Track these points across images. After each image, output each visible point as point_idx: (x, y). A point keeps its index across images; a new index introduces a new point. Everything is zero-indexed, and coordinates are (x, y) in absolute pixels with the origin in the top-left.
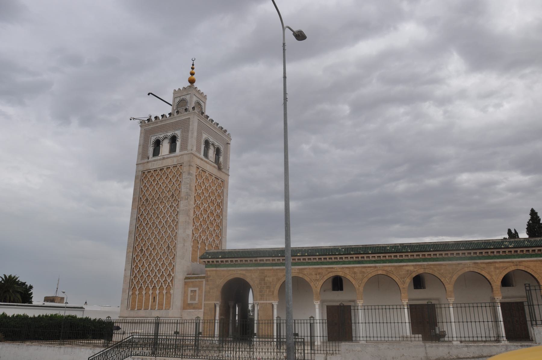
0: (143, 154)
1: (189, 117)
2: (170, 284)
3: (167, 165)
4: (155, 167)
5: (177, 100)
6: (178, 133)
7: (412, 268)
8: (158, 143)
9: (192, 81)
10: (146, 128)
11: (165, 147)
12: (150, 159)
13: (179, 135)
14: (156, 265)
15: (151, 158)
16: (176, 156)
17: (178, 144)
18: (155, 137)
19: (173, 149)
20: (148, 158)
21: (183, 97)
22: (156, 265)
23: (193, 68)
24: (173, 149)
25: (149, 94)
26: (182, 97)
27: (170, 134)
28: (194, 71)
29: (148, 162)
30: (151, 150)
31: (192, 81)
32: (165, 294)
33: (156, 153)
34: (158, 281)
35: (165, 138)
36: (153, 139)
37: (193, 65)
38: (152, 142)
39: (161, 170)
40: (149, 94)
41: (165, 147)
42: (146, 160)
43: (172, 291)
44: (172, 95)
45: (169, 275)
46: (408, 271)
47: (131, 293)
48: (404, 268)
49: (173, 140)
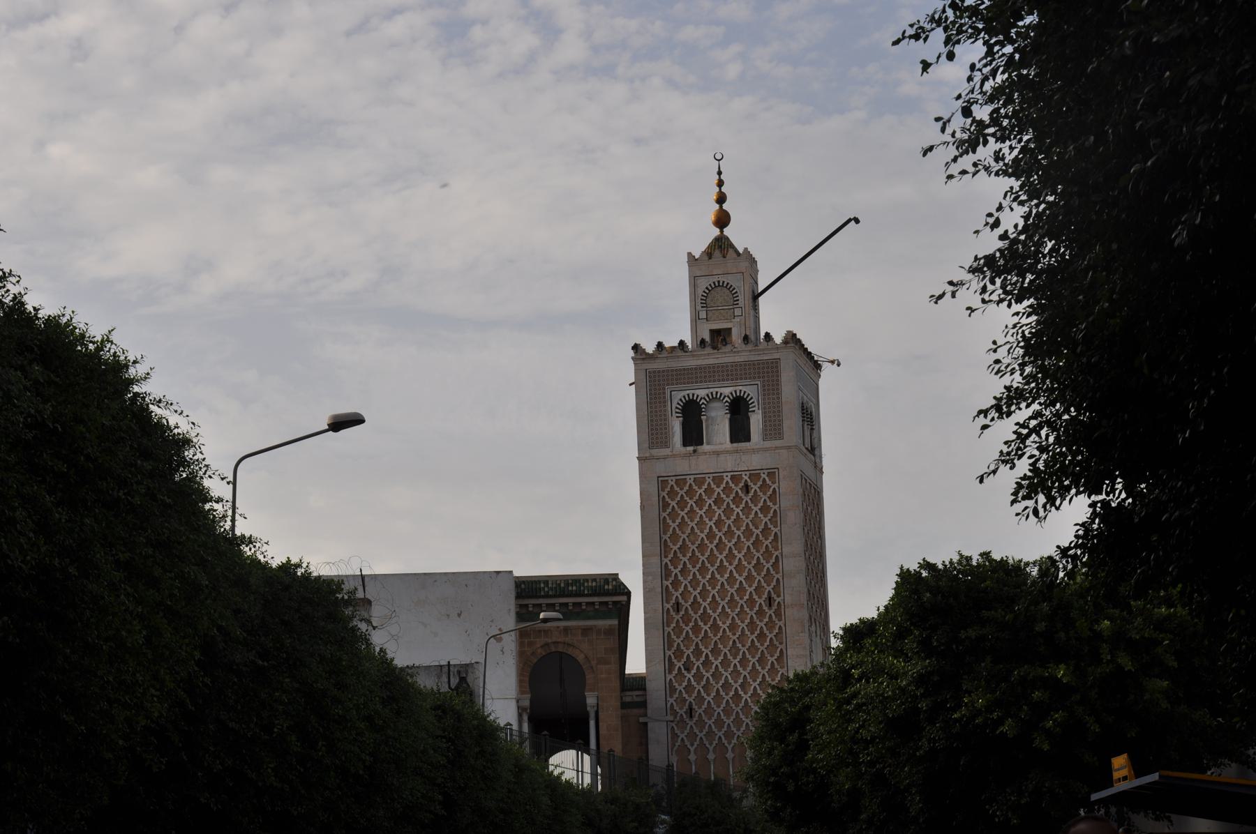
0: (652, 434)
1: (776, 356)
6: (750, 390)
8: (692, 414)
9: (722, 220)
11: (718, 424)
16: (754, 451)
17: (756, 421)
19: (740, 432)
23: (720, 183)
24: (740, 432)
28: (723, 189)
29: (674, 456)
30: (676, 426)
31: (722, 220)
33: (693, 435)
36: (679, 396)
37: (720, 173)
41: (718, 424)
49: (738, 408)
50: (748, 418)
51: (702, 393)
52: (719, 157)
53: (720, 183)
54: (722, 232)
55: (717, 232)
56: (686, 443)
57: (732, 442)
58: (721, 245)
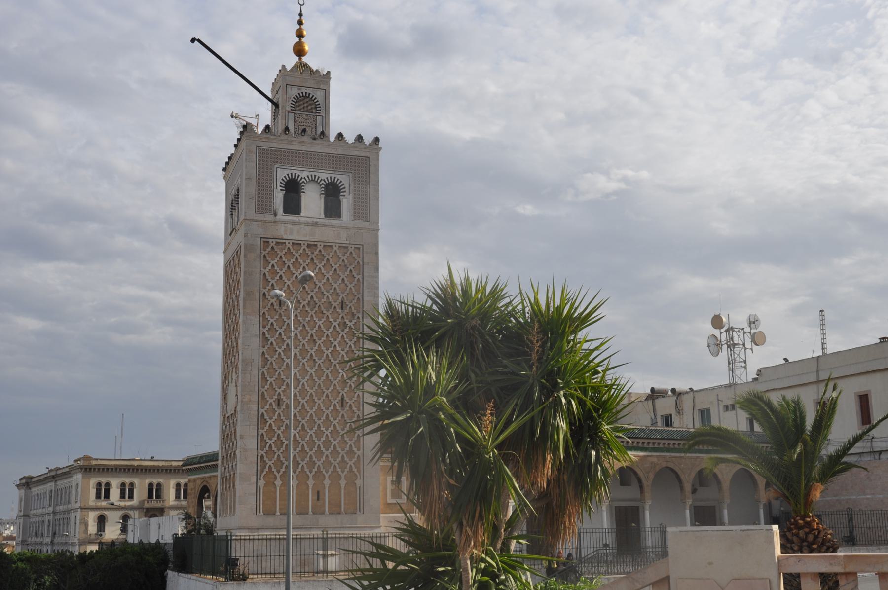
2: (355, 470)
3: (325, 239)
4: (295, 237)
5: (294, 92)
6: (344, 179)
7: (655, 460)
8: (293, 188)
9: (299, 51)
10: (262, 144)
11: (312, 201)
12: (278, 217)
13: (346, 185)
14: (319, 433)
15: (281, 216)
17: (346, 203)
18: (286, 172)
19: (332, 209)
20: (276, 215)
21: (308, 91)
22: (319, 433)
23: (300, 23)
25: (193, 40)
26: (304, 90)
27: (324, 175)
30: (279, 196)
31: (299, 51)
32: (343, 486)
33: (292, 205)
34: (327, 463)
35: (314, 180)
36: (282, 174)
37: (301, 15)
38: (279, 180)
39: (309, 246)
40: (193, 40)
41: (312, 201)
42: (270, 217)
43: (359, 482)
44: (273, 75)
45: (351, 452)
46: (652, 463)
47: (262, 483)
48: (649, 459)
50: (339, 203)
51: (304, 174)
52: (302, 3)
53: (300, 23)
54: (300, 59)
55: (297, 59)
56: (287, 210)
57: (326, 216)
58: (302, 67)
